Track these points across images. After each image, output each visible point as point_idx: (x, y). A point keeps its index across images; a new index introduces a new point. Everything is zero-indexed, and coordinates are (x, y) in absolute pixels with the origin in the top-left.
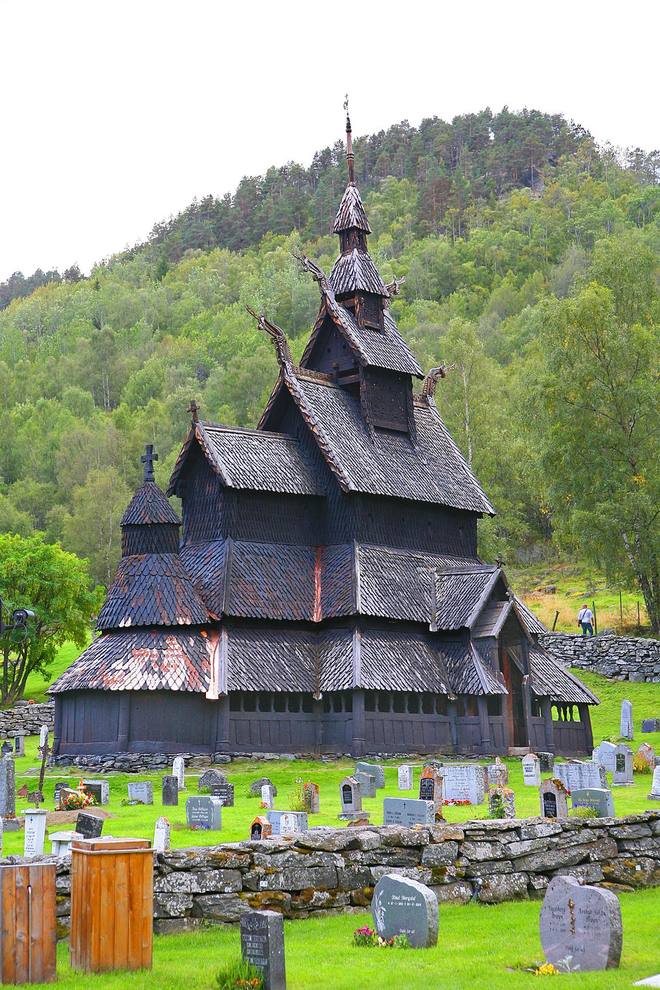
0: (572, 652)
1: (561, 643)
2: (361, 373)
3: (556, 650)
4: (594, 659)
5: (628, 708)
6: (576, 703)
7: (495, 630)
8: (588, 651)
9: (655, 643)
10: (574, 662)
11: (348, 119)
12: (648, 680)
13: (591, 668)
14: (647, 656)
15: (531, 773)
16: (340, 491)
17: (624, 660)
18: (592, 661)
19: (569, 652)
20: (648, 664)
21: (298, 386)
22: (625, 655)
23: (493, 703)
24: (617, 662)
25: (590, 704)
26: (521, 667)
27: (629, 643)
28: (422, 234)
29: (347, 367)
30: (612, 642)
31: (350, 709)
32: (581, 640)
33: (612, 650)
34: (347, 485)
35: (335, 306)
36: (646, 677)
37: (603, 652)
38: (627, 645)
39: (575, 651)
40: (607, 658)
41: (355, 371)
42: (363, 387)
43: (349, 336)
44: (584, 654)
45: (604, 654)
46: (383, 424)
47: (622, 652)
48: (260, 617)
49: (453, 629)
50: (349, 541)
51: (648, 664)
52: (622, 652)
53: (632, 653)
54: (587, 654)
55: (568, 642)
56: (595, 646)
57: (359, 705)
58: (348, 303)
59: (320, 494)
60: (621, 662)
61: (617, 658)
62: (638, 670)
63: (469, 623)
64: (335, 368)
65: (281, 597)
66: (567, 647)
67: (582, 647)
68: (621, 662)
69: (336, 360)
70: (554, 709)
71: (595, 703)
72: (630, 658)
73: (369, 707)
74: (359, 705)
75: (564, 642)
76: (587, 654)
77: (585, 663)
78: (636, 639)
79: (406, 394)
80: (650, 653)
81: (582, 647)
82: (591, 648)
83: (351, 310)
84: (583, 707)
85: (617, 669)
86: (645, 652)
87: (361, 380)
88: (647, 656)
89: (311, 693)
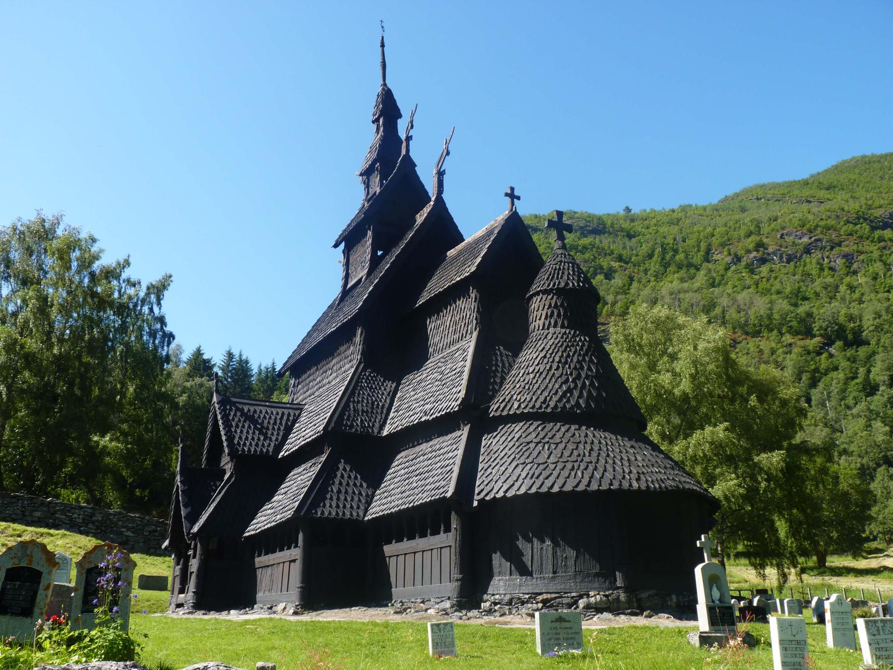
0: (81, 521)
4: (103, 528)
8: (98, 521)
11: (383, 37)
17: (132, 532)
22: (133, 528)
33: (121, 523)
36: (150, 548)
44: (93, 523)
54: (97, 524)
55: (77, 511)
60: (129, 533)
61: (125, 530)
67: (91, 517)
68: (129, 533)
75: (73, 511)
80: (159, 529)
85: (124, 539)
88: (155, 531)
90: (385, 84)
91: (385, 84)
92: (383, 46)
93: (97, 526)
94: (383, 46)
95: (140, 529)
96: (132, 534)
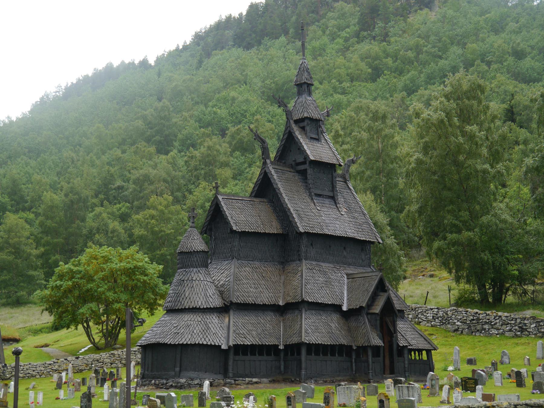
0: (431, 318)
1: (425, 312)
2: (308, 164)
3: (423, 316)
4: (444, 321)
5: (457, 352)
6: (424, 350)
8: (440, 317)
9: (477, 313)
10: (432, 323)
12: (474, 334)
13: (442, 327)
14: (473, 320)
15: (389, 390)
16: (295, 231)
17: (461, 322)
18: (443, 323)
19: (430, 318)
20: (474, 325)
21: (273, 172)
22: (461, 319)
23: (376, 349)
24: (457, 324)
25: (432, 350)
26: (392, 329)
27: (463, 312)
28: (360, 40)
29: (301, 160)
30: (454, 311)
31: (299, 354)
32: (436, 310)
33: (454, 316)
35: (293, 126)
36: (472, 332)
37: (449, 318)
38: (462, 313)
39: (433, 317)
40: (451, 321)
41: (304, 163)
42: (309, 172)
43: (301, 143)
44: (438, 318)
45: (449, 319)
46: (319, 192)
47: (459, 317)
48: (250, 303)
50: (300, 260)
51: (474, 325)
52: (459, 317)
53: (465, 318)
54: (440, 319)
55: (429, 311)
56: (444, 314)
57: (304, 351)
58: (302, 125)
59: (284, 233)
60: (459, 323)
61: (456, 321)
62: (468, 328)
64: (294, 161)
65: (262, 291)
66: (429, 315)
67: (437, 315)
68: (459, 323)
69: (293, 157)
70: (413, 353)
71: (435, 349)
72: (463, 322)
73: (309, 353)
74: (304, 351)
76: (440, 319)
77: (438, 324)
78: (467, 310)
79: (332, 175)
80: (475, 318)
81: (437, 315)
82: (442, 315)
83: (303, 128)
84: (429, 352)
85: (457, 327)
86: (472, 317)
87: (308, 168)
88: (473, 320)
93: (440, 320)
95: (465, 320)
96: (460, 324)
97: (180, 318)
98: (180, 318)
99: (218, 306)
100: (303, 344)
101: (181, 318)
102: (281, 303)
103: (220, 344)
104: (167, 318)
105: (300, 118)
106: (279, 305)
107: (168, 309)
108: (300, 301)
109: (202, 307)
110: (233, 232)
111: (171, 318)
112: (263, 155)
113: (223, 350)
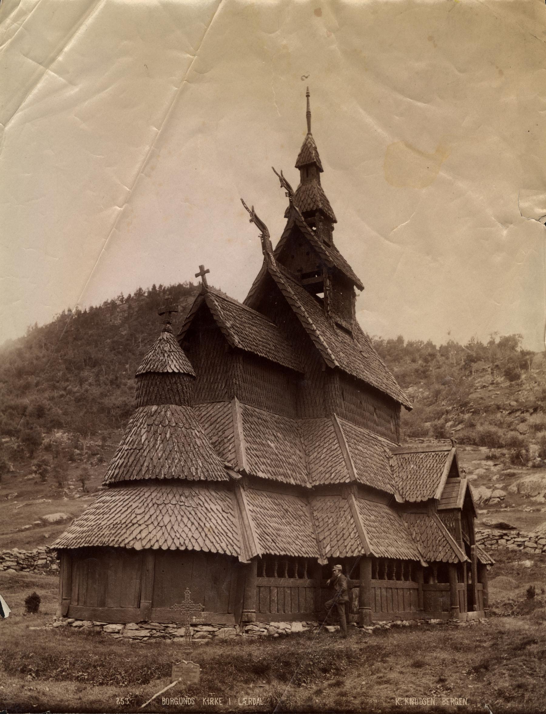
7: (460, 503)
34: (332, 361)
49: (422, 501)
63: (438, 496)
89: (317, 558)
90: (309, 133)
91: (309, 133)
92: (308, 96)
94: (308, 96)
97: (147, 498)
98: (147, 498)
99: (220, 480)
100: (372, 557)
101: (150, 499)
102: (309, 486)
103: (235, 554)
104: (117, 497)
105: (309, 210)
106: (305, 488)
107: (117, 480)
108: (347, 481)
109: (190, 478)
110: (235, 352)
111: (127, 497)
112: (263, 250)
113: (242, 563)
